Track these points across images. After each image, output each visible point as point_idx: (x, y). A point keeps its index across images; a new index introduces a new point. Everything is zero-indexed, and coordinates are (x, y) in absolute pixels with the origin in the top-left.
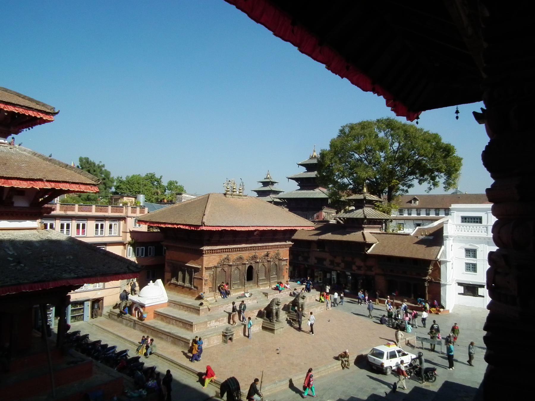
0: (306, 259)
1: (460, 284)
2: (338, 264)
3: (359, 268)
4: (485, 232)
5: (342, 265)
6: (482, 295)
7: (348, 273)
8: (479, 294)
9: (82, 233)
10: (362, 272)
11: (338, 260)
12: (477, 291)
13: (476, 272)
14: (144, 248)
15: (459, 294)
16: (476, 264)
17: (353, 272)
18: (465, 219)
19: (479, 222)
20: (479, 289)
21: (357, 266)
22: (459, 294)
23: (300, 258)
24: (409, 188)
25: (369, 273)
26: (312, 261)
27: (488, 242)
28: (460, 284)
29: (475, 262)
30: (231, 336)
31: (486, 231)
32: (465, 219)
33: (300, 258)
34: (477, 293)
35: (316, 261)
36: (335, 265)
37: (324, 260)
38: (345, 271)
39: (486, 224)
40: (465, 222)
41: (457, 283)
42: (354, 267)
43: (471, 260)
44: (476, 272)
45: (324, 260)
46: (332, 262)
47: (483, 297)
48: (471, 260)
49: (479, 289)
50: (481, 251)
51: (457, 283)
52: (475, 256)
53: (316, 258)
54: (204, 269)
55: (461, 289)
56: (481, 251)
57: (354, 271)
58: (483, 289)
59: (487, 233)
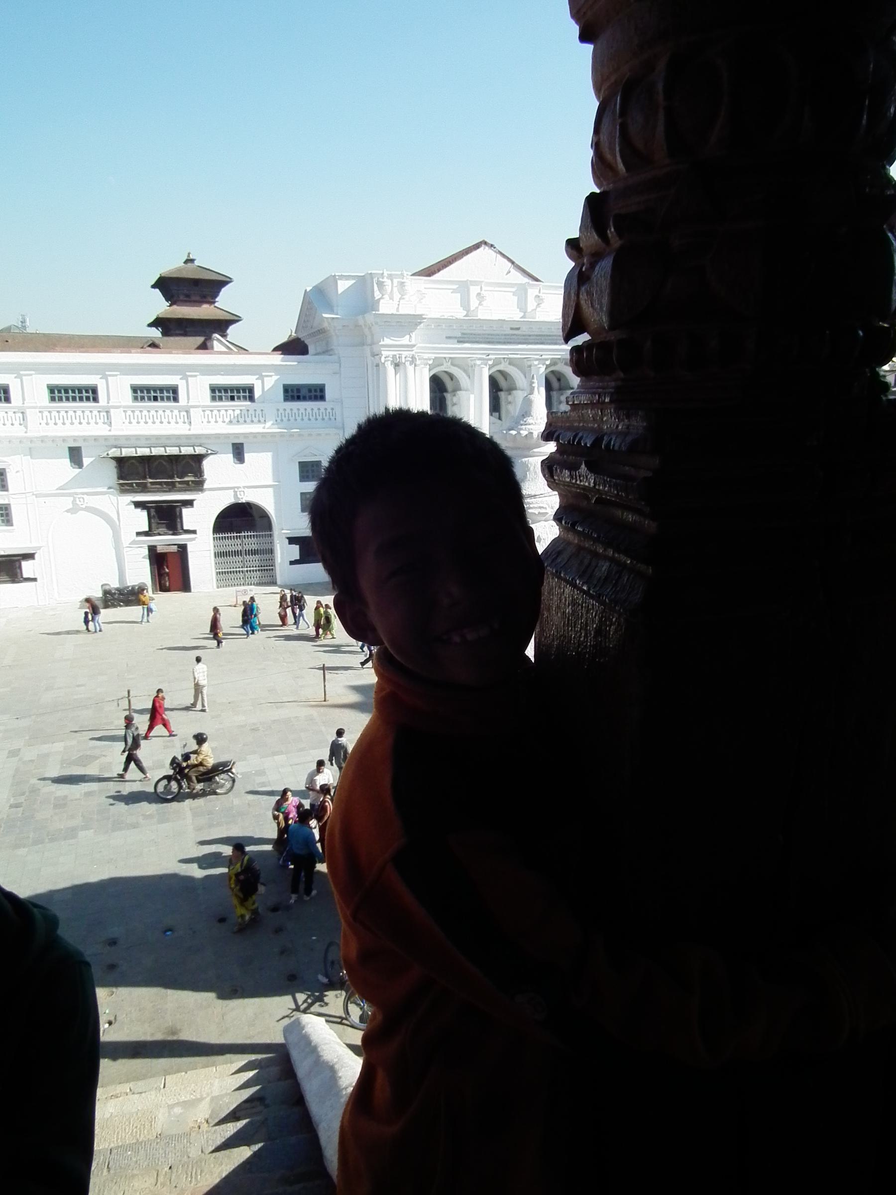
4: (20, 424)
6: (32, 576)
8: (25, 576)
12: (18, 571)
13: (12, 525)
16: (9, 504)
27: (30, 448)
29: (6, 502)
31: (22, 422)
34: (19, 575)
39: (20, 404)
44: (12, 525)
47: (35, 580)
49: (25, 564)
50: (17, 472)
56: (17, 472)
59: (26, 427)
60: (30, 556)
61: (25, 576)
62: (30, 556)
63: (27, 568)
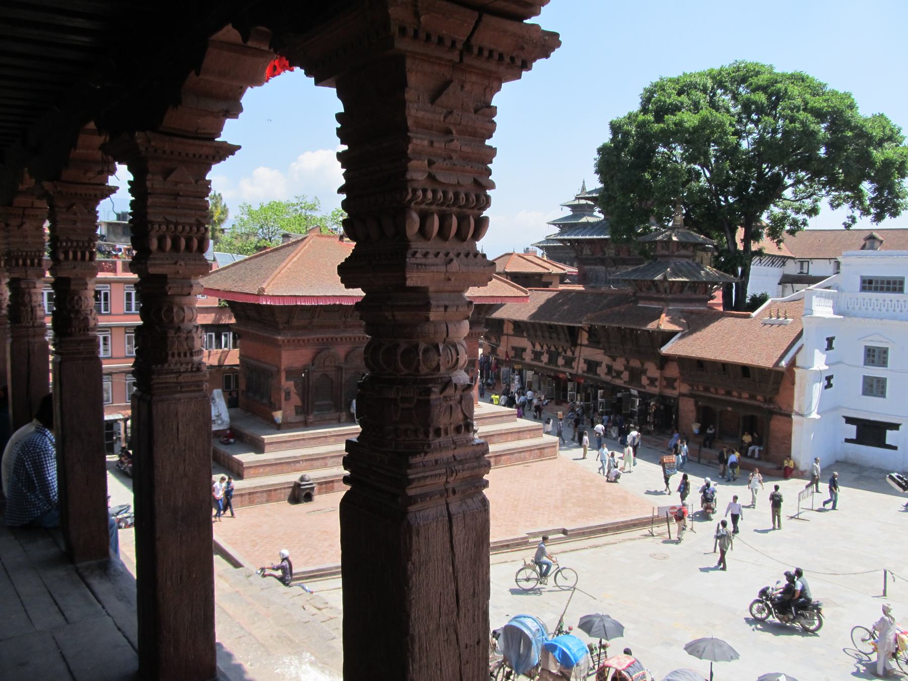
0: (569, 362)
1: (849, 420)
2: (619, 374)
3: (652, 381)
5: (626, 375)
7: (634, 392)
8: (887, 442)
9: (131, 306)
10: (655, 390)
11: (619, 365)
14: (214, 334)
15: (847, 441)
17: (642, 390)
18: (869, 284)
19: (885, 289)
20: (889, 432)
21: (649, 378)
22: (847, 441)
23: (561, 361)
24: (810, 216)
25: (669, 392)
26: (580, 367)
28: (849, 420)
30: (308, 491)
32: (869, 284)
33: (561, 361)
35: (585, 367)
36: (614, 374)
37: (598, 364)
38: (629, 387)
40: (870, 290)
41: (844, 417)
42: (644, 381)
43: (876, 372)
45: (598, 364)
46: (610, 369)
47: (895, 448)
48: (876, 372)
49: (889, 432)
51: (844, 417)
52: (884, 363)
53: (587, 361)
54: (283, 375)
55: (852, 431)
57: (644, 387)
58: (894, 432)
60: (895, 427)
61: (887, 442)
62: (895, 427)
63: (891, 437)
